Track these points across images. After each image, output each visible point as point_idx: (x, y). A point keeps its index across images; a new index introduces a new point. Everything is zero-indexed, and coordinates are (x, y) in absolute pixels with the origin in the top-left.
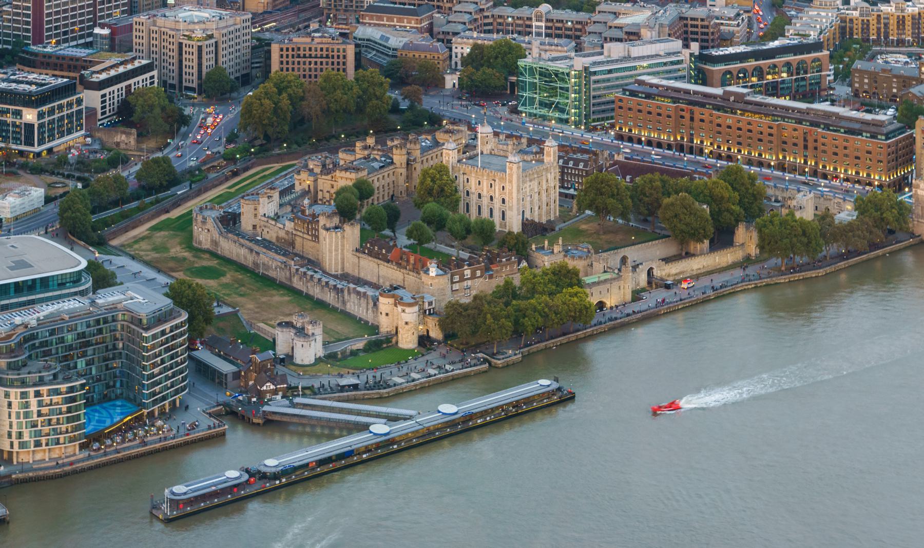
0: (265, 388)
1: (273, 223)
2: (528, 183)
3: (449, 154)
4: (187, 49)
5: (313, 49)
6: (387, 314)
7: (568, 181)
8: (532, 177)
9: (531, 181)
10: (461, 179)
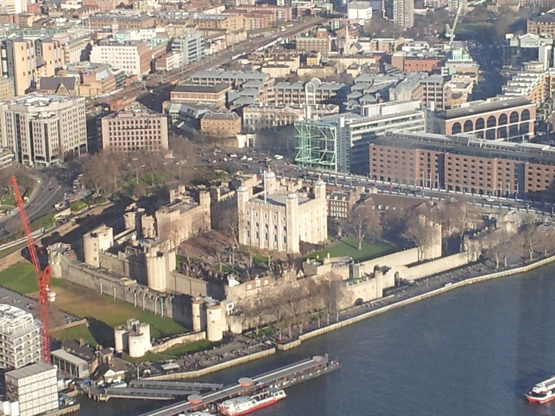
7: (333, 212)
9: (305, 212)
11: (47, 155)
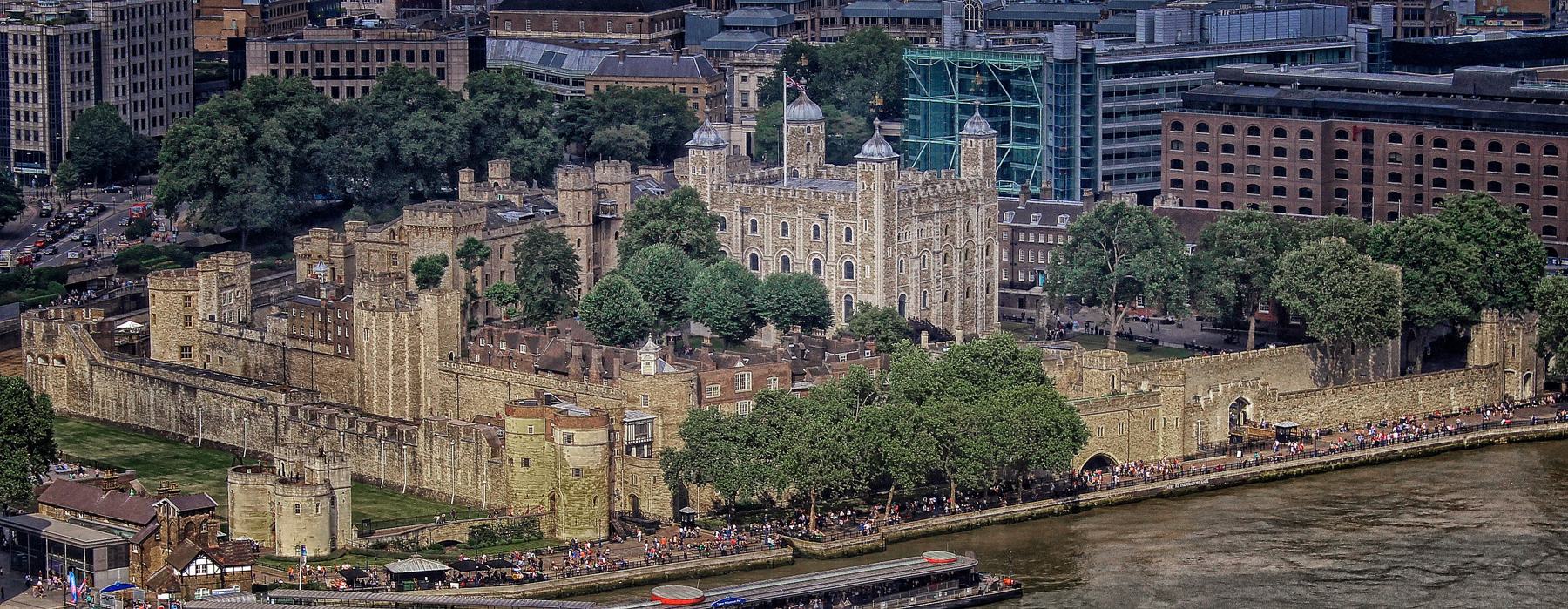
0: (192, 570)
1: (235, 332)
2: (915, 225)
3: (703, 161)
4: (21, 88)
5: (358, 55)
6: (526, 463)
7: (1026, 267)
8: (925, 209)
9: (922, 218)
10: (735, 225)
11: (55, 146)
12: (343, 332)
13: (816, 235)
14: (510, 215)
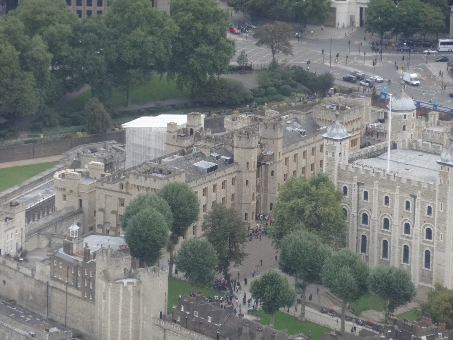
1: (14, 265)
3: (334, 148)
10: (353, 194)
12: (88, 284)
13: (408, 207)
14: (203, 164)
